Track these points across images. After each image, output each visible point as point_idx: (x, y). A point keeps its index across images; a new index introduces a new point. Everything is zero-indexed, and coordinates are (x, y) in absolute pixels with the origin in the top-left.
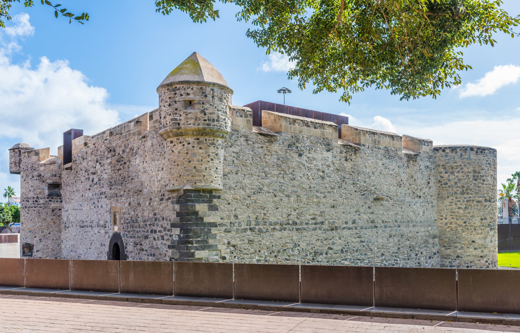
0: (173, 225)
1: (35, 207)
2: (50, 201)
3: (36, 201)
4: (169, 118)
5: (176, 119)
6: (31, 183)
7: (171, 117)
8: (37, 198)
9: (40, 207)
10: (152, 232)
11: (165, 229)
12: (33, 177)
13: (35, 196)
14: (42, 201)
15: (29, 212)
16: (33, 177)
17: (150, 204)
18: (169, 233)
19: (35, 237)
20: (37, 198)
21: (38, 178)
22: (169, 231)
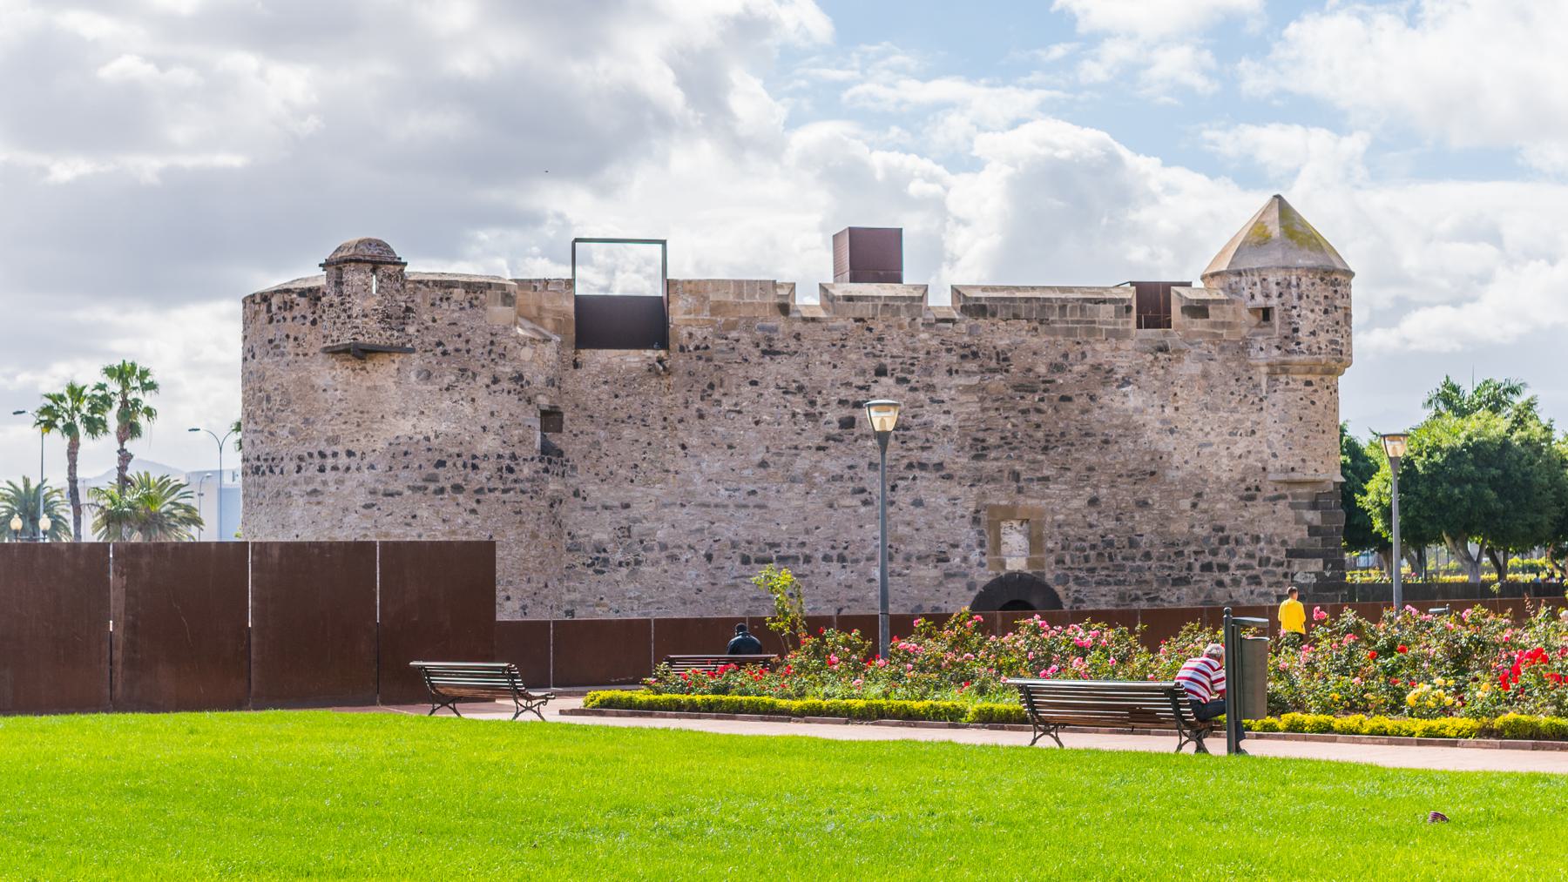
0: (1292, 554)
1: (505, 491)
2: (546, 470)
3: (510, 470)
4: (1323, 338)
5: (1336, 343)
6: (484, 401)
7: (1330, 336)
8: (513, 457)
9: (523, 492)
10: (1207, 567)
11: (1264, 562)
12: (496, 381)
13: (507, 452)
14: (526, 471)
15: (481, 509)
16: (496, 381)
17: (1194, 505)
18: (1280, 570)
19: (508, 598)
20: (513, 457)
21: (512, 386)
22: (1279, 564)
